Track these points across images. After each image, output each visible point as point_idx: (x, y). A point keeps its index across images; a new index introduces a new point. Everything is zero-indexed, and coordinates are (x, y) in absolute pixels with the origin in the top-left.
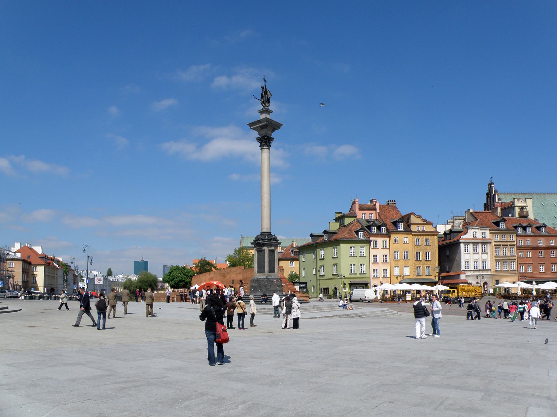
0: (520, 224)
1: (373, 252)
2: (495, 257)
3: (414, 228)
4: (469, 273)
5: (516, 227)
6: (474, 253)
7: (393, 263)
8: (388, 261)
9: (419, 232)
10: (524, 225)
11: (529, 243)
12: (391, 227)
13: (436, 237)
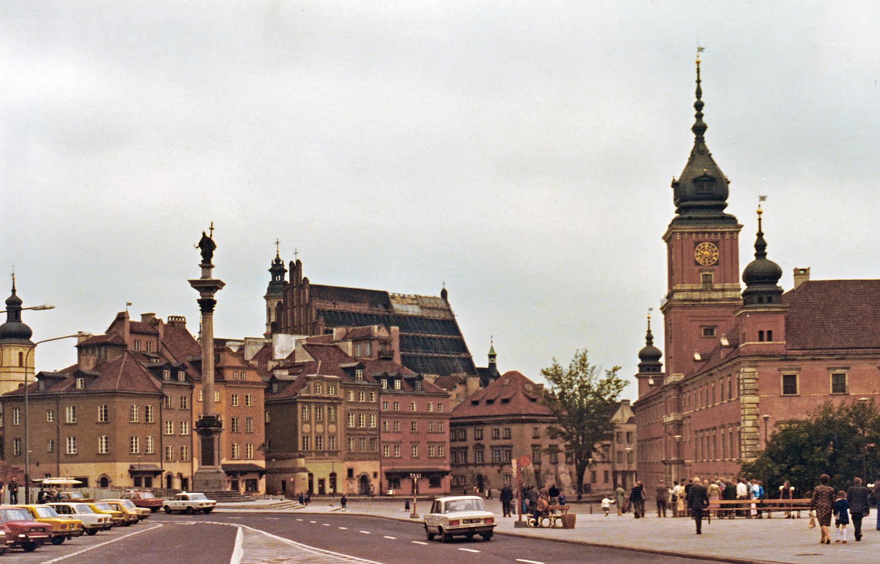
0: (386, 373)
3: (229, 375)
5: (378, 379)
9: (236, 382)
10: (391, 375)
12: (191, 371)
13: (262, 392)
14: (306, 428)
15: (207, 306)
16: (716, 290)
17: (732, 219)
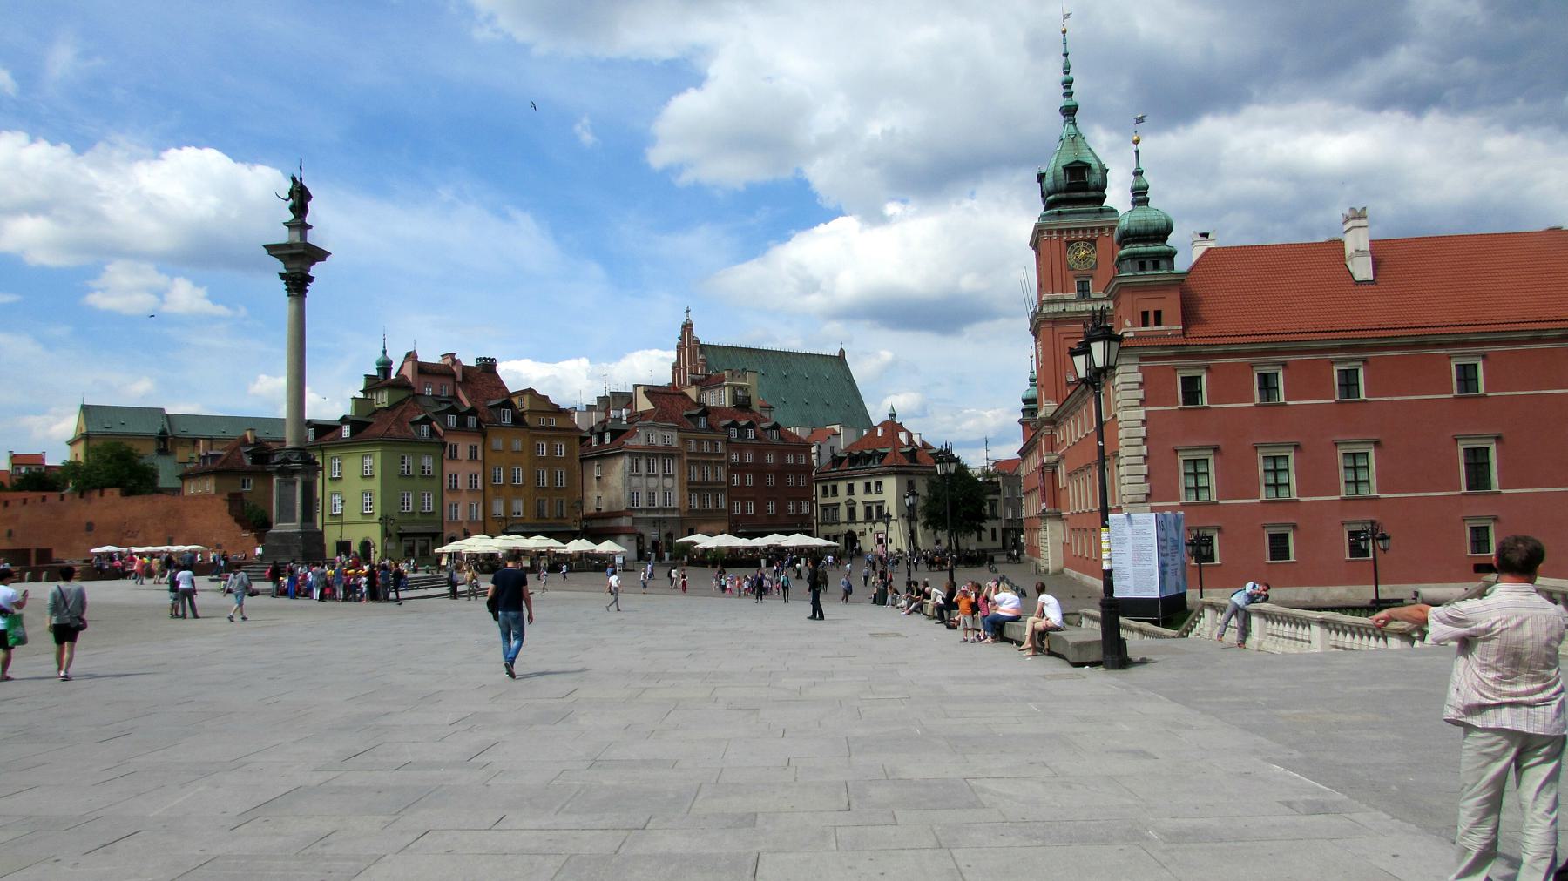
1: (450, 467)
2: (689, 483)
4: (639, 515)
5: (726, 427)
6: (648, 476)
7: (490, 492)
8: (480, 486)
9: (543, 428)
10: (743, 423)
11: (749, 458)
13: (577, 441)
14: (635, 481)
15: (298, 284)
16: (1095, 300)
17: (1112, 211)
